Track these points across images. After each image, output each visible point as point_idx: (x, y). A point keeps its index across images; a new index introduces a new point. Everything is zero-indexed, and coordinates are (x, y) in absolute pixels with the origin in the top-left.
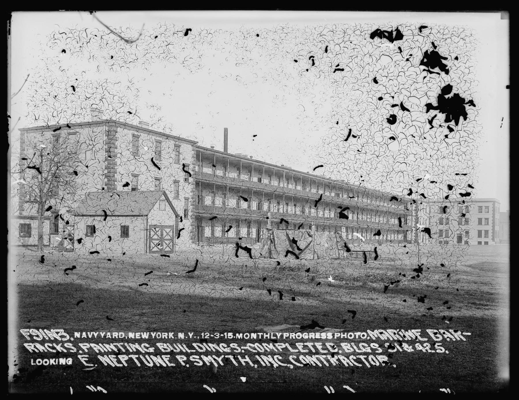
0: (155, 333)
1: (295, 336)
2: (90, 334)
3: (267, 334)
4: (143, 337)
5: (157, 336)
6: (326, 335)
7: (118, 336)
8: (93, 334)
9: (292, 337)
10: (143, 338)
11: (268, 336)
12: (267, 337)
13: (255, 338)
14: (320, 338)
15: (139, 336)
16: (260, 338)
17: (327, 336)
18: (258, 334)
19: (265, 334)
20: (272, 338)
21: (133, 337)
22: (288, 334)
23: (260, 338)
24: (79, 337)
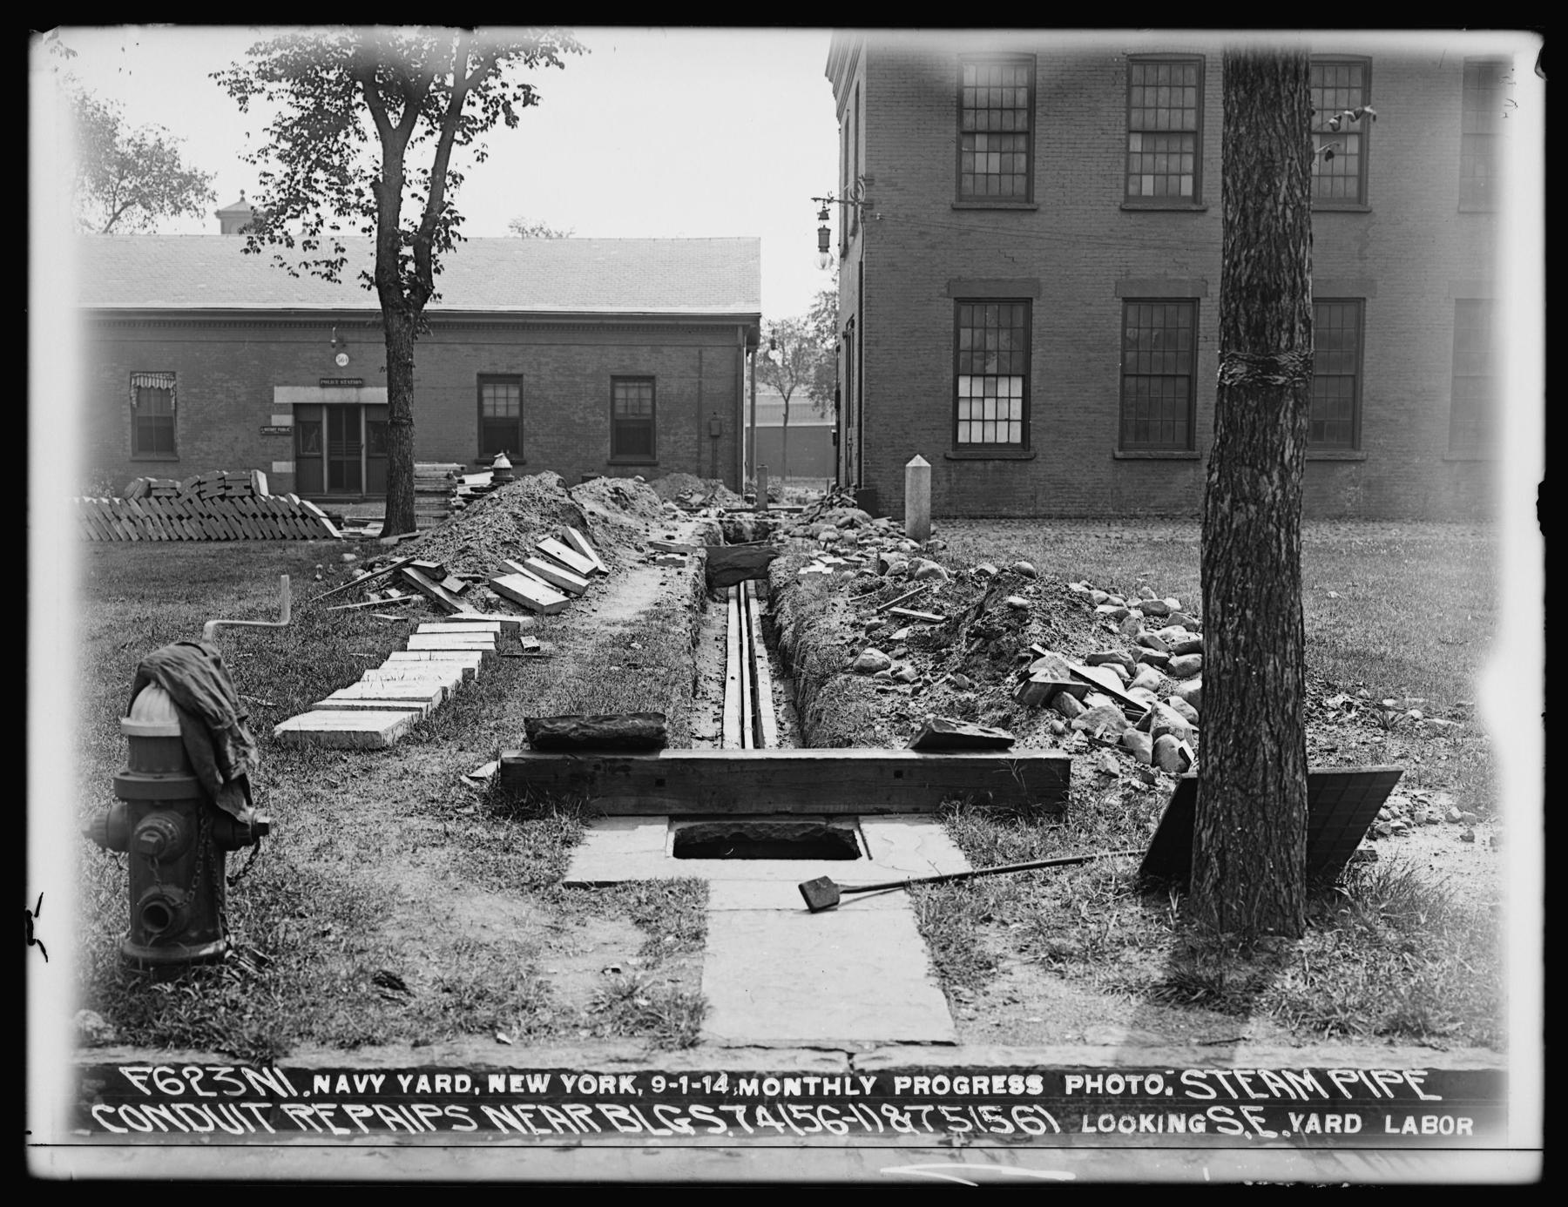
0: (574, 1078)
1: (930, 1086)
2: (361, 1081)
3: (832, 1081)
4: (533, 1089)
5: (581, 1086)
6: (1024, 1082)
7: (453, 1085)
8: (370, 1084)
9: (921, 1090)
10: (533, 1089)
11: (836, 1087)
12: (832, 1092)
13: (797, 1092)
14: (1004, 1091)
15: (519, 1084)
16: (812, 1091)
17: (1027, 1087)
18: (806, 1080)
19: (826, 1081)
21: (502, 1089)
22: (908, 1080)
23: (812, 1091)
24: (326, 1090)
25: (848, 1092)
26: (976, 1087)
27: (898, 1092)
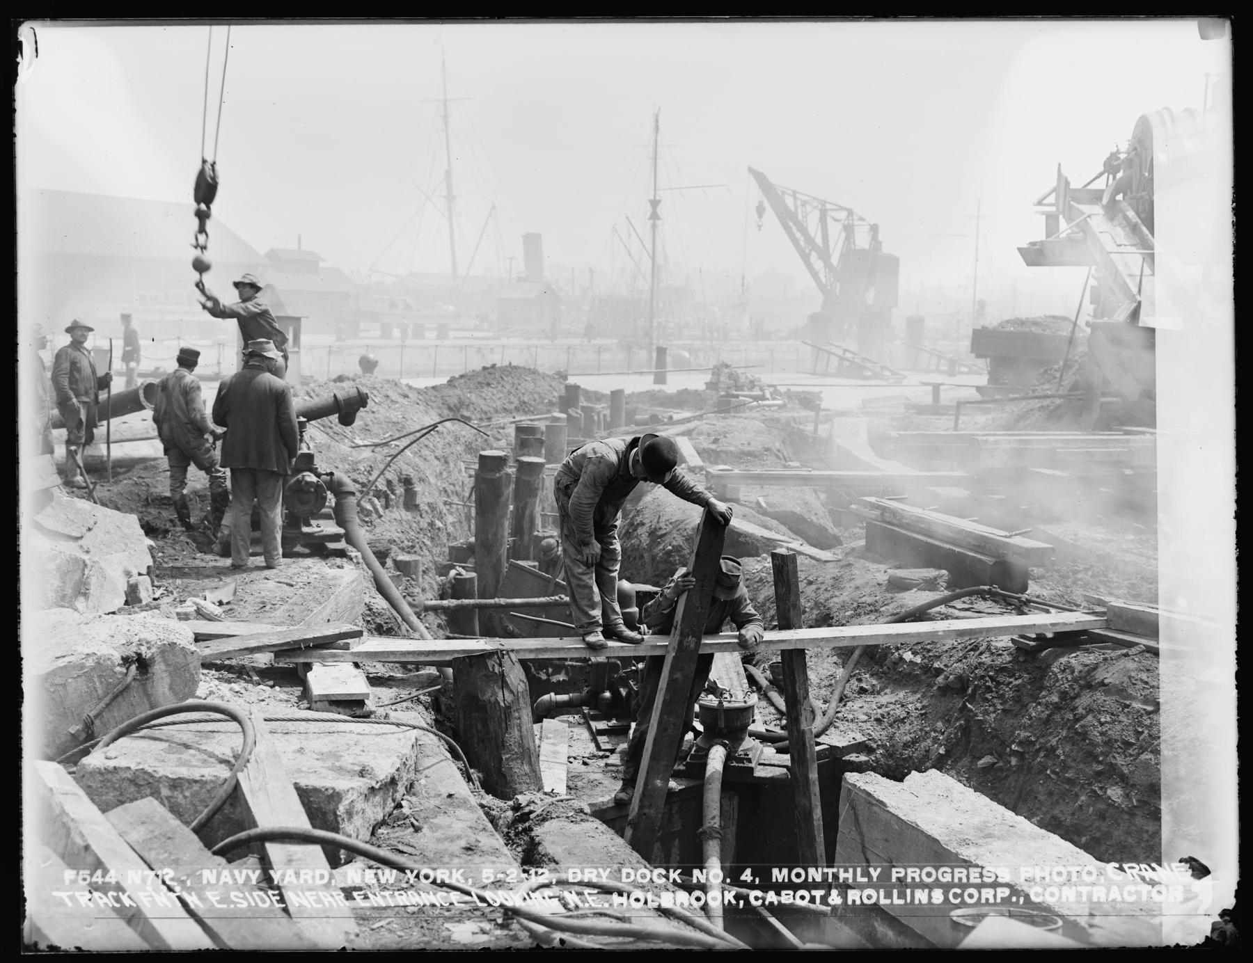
1: (920, 876)
9: (913, 878)
13: (819, 879)
19: (841, 870)
20: (859, 879)
25: (859, 879)
26: (957, 876)
27: (894, 880)
